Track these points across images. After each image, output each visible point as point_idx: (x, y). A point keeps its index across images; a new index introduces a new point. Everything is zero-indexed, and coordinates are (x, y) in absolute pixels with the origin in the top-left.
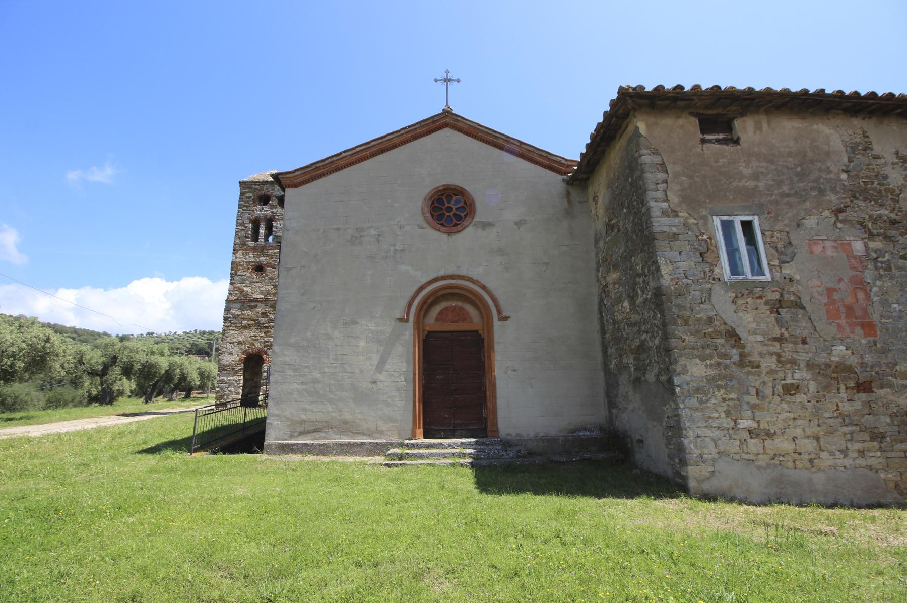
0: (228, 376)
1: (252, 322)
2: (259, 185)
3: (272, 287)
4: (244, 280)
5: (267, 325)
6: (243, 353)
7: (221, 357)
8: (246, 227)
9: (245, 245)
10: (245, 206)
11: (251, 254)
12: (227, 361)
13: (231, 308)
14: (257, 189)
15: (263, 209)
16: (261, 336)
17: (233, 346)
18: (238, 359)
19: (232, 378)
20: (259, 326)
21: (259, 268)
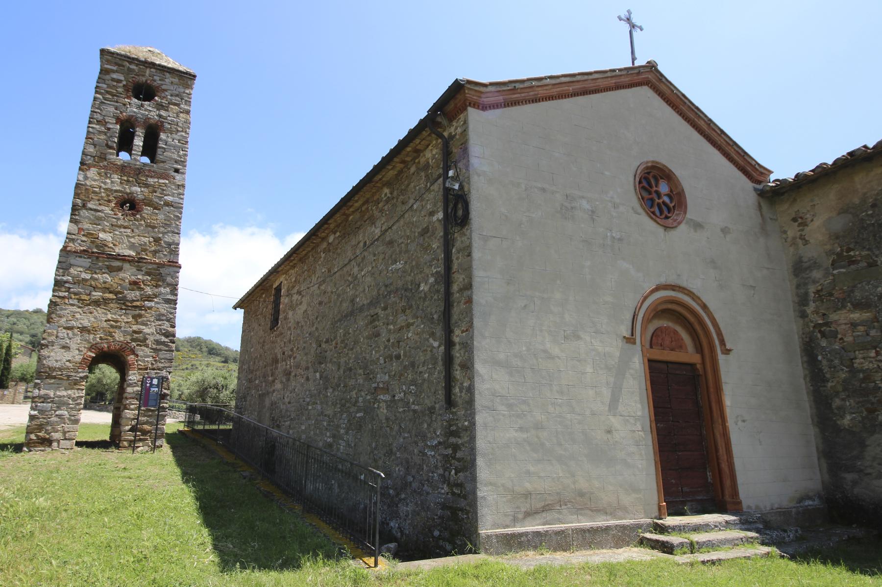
0: (57, 389)
2: (137, 65)
3: (151, 239)
4: (100, 219)
5: (138, 303)
6: (90, 349)
7: (45, 352)
8: (109, 129)
9: (105, 159)
11: (116, 178)
12: (57, 361)
13: (71, 265)
14: (133, 70)
15: (142, 105)
16: (127, 322)
17: (71, 335)
18: (78, 358)
19: (65, 393)
20: (124, 304)
21: (130, 205)
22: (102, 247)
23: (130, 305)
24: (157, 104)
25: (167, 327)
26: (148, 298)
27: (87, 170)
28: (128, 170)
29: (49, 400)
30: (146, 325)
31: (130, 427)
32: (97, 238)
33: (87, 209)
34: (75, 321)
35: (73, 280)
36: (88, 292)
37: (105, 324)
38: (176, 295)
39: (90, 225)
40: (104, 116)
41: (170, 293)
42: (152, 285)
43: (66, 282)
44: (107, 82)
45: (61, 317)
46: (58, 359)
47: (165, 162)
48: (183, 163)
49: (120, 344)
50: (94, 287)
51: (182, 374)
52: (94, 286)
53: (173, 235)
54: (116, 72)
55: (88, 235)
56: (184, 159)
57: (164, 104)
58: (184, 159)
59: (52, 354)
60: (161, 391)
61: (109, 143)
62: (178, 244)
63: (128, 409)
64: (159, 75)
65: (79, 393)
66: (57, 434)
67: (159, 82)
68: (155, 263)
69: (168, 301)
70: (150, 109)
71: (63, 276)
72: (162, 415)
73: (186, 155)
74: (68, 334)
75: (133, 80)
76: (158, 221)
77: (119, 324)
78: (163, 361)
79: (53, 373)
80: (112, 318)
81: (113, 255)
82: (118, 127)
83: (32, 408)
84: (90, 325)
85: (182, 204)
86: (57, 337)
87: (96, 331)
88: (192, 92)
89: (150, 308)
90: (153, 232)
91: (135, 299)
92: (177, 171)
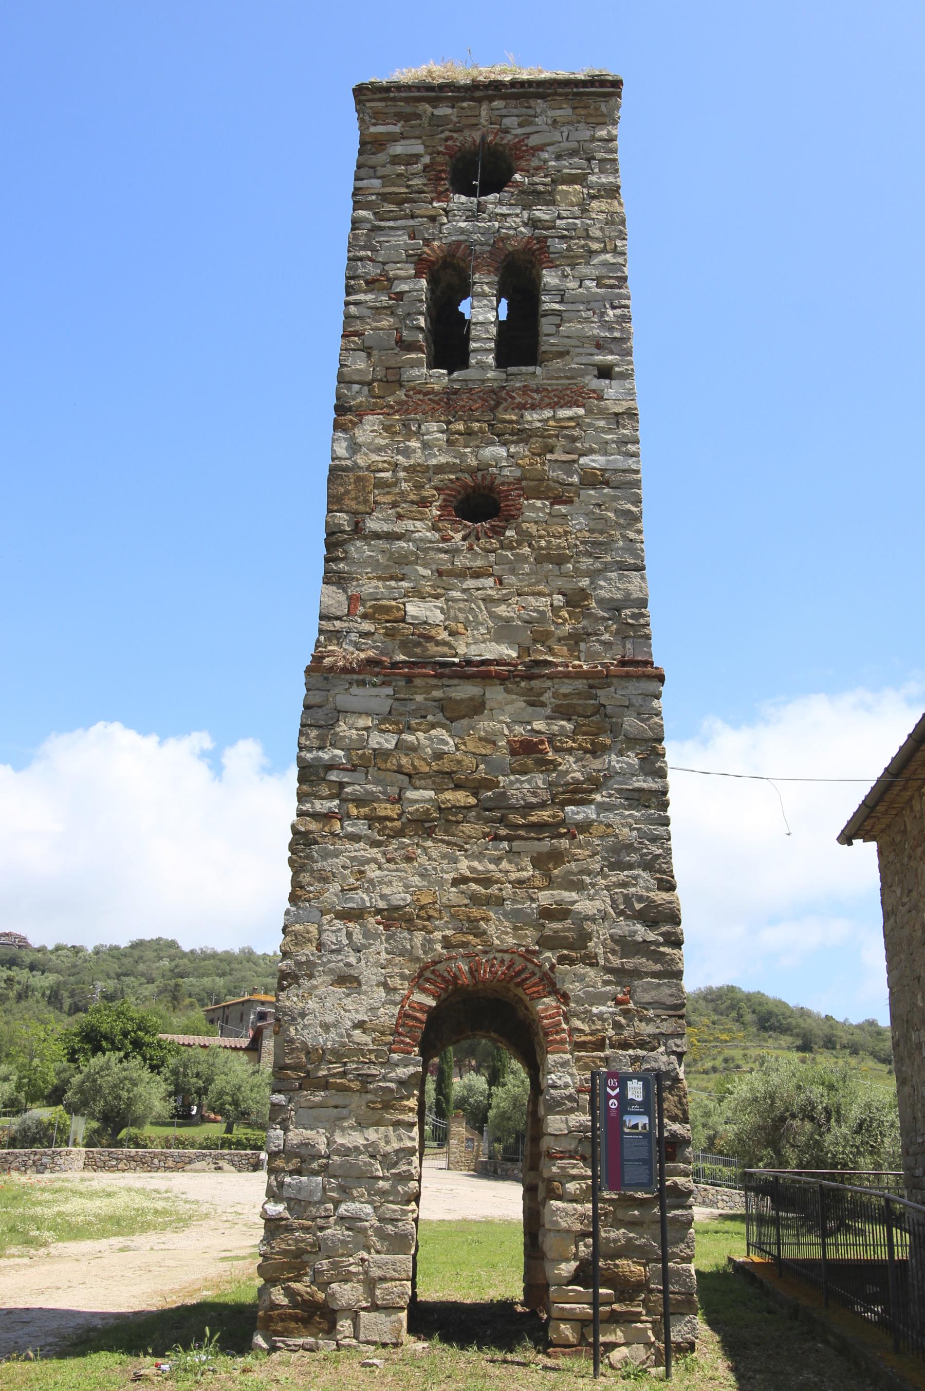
0: (334, 1125)
1: (462, 798)
3: (559, 600)
4: (402, 560)
5: (545, 815)
6: (418, 981)
8: (400, 296)
9: (400, 384)
10: (385, 197)
11: (434, 430)
12: (326, 1027)
13: (340, 712)
15: (481, 208)
16: (520, 882)
17: (358, 937)
18: (388, 1015)
19: (355, 1139)
20: (501, 820)
22: (418, 644)
23: (521, 821)
24: (522, 192)
25: (648, 889)
26: (574, 792)
27: (355, 424)
28: (464, 400)
29: (315, 1165)
30: (579, 887)
31: (574, 1265)
32: (403, 620)
33: (365, 538)
34: (367, 891)
35: (348, 757)
36: (393, 791)
37: (453, 895)
38: (662, 774)
39: (380, 584)
40: (384, 264)
41: (641, 768)
42: (580, 748)
43: (330, 767)
44: (381, 171)
45: (325, 880)
46: (330, 1019)
47: (568, 353)
48: (621, 345)
49: (507, 957)
50: (409, 776)
51: (704, 1084)
52: (408, 768)
53: (621, 577)
54: (403, 136)
55: (377, 613)
56: (622, 330)
57: (541, 188)
58: (622, 330)
59: (312, 1004)
60: (662, 1126)
61: (405, 333)
62: (643, 603)
63: (560, 1198)
64: (515, 111)
65: (400, 1139)
66: (348, 1286)
67: (520, 131)
68: (580, 675)
69: (637, 799)
70: (504, 210)
71: (321, 748)
72: (675, 1219)
73: (626, 319)
74: (349, 935)
75: (447, 147)
76: (572, 539)
77: (494, 890)
78: (651, 1013)
79: (318, 1068)
80: (472, 869)
81: (454, 664)
82: (424, 283)
83: (273, 1195)
84: (409, 898)
85: (637, 472)
86: (320, 946)
87: (429, 918)
88: (614, 132)
89: (585, 827)
90: (562, 575)
91: (534, 800)
92: (605, 372)
